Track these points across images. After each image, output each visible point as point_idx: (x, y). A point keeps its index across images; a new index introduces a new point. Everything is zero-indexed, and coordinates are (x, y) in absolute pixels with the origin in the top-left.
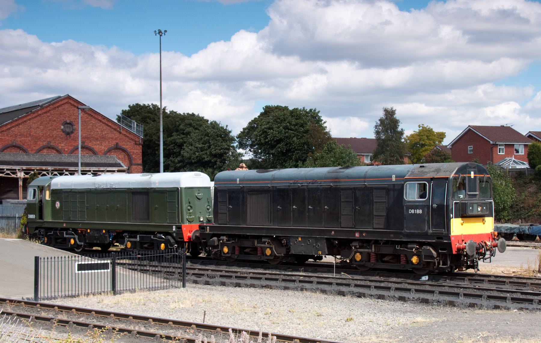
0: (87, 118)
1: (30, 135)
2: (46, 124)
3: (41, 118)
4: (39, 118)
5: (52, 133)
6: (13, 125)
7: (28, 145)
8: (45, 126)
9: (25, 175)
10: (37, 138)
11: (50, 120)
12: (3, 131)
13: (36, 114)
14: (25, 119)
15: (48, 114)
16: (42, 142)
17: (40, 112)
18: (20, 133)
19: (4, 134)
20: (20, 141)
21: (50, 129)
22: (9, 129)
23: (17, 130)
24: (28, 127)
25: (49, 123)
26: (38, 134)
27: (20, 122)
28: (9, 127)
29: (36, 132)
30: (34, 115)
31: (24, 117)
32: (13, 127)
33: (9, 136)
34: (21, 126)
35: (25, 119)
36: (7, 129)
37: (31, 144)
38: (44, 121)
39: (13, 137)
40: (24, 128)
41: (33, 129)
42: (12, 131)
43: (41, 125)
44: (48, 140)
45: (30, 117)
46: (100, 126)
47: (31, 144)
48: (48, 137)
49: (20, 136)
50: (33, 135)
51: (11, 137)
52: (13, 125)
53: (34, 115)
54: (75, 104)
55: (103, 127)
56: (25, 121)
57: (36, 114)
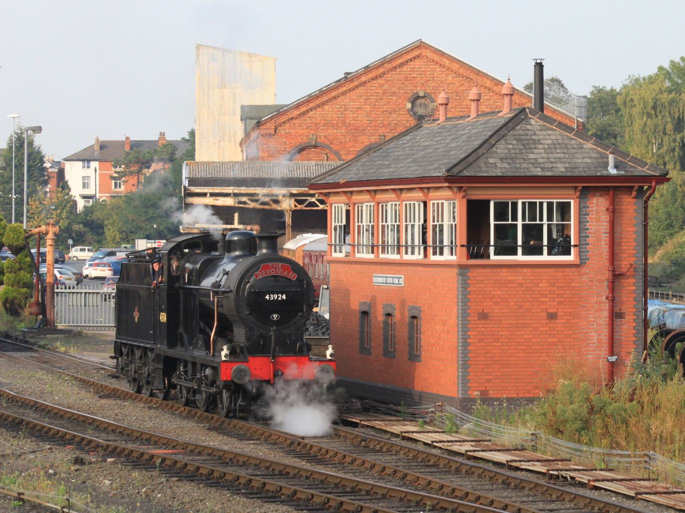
0: (462, 85)
1: (344, 123)
2: (377, 100)
3: (367, 90)
4: (361, 90)
5: (388, 117)
6: (311, 105)
7: (341, 143)
8: (375, 105)
9: (297, 204)
10: (358, 130)
11: (384, 93)
12: (292, 118)
13: (356, 83)
14: (334, 94)
15: (381, 81)
16: (368, 136)
17: (363, 79)
18: (324, 120)
19: (295, 124)
20: (325, 137)
21: (384, 111)
22: (304, 113)
23: (320, 114)
24: (341, 108)
25: (382, 99)
26: (361, 121)
27: (325, 98)
28: (303, 109)
29: (357, 117)
30: (352, 85)
31: (332, 90)
32: (311, 109)
33: (305, 127)
34: (326, 107)
35: (334, 94)
36: (300, 114)
37: (345, 142)
38: (372, 95)
39: (311, 129)
40: (332, 111)
41: (351, 111)
42: (309, 117)
43: (366, 104)
44: (381, 131)
45: (344, 89)
46: (488, 100)
47: (345, 142)
48: (381, 127)
49: (324, 126)
50: (350, 124)
51: (306, 129)
52: (311, 105)
53: (352, 85)
54: (436, 58)
55: (495, 102)
56: (335, 98)
57: (356, 83)
